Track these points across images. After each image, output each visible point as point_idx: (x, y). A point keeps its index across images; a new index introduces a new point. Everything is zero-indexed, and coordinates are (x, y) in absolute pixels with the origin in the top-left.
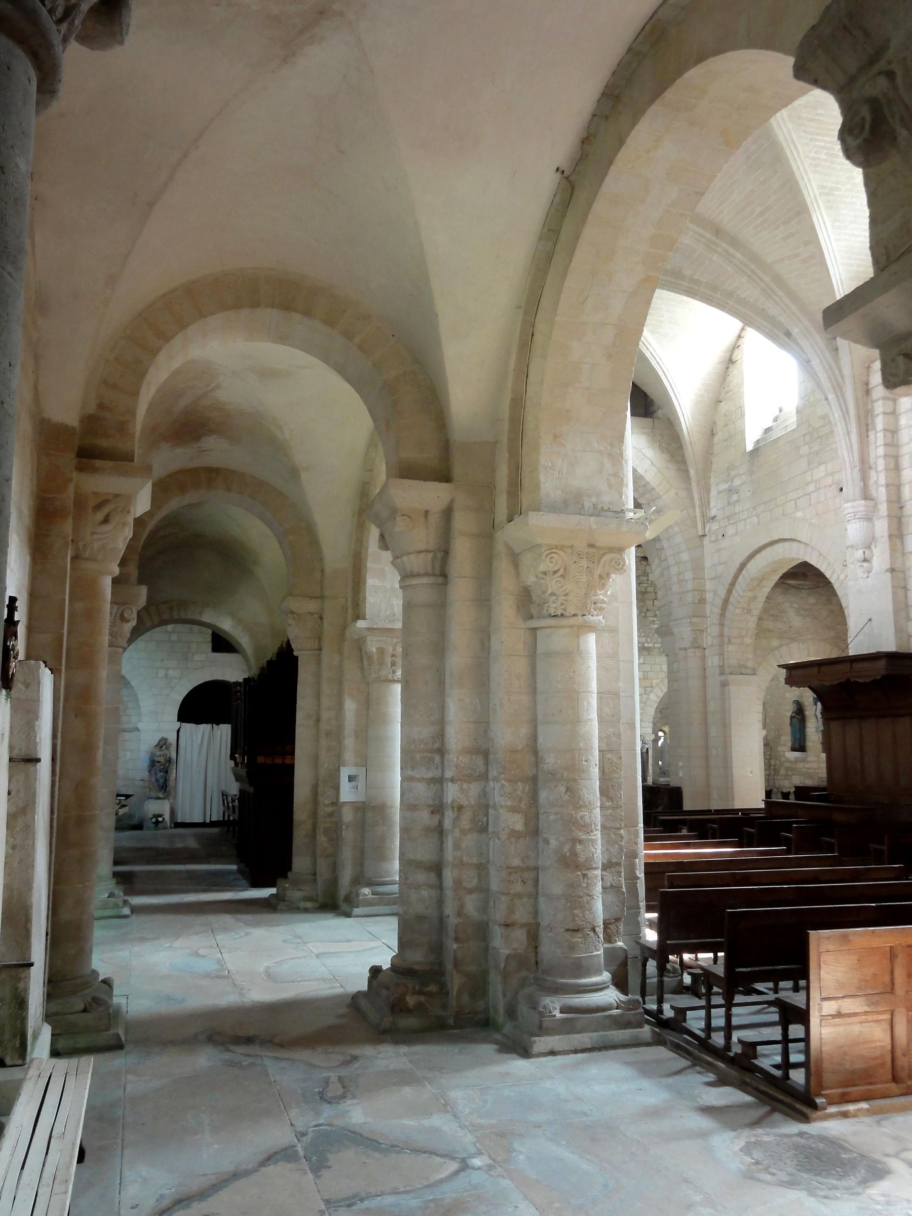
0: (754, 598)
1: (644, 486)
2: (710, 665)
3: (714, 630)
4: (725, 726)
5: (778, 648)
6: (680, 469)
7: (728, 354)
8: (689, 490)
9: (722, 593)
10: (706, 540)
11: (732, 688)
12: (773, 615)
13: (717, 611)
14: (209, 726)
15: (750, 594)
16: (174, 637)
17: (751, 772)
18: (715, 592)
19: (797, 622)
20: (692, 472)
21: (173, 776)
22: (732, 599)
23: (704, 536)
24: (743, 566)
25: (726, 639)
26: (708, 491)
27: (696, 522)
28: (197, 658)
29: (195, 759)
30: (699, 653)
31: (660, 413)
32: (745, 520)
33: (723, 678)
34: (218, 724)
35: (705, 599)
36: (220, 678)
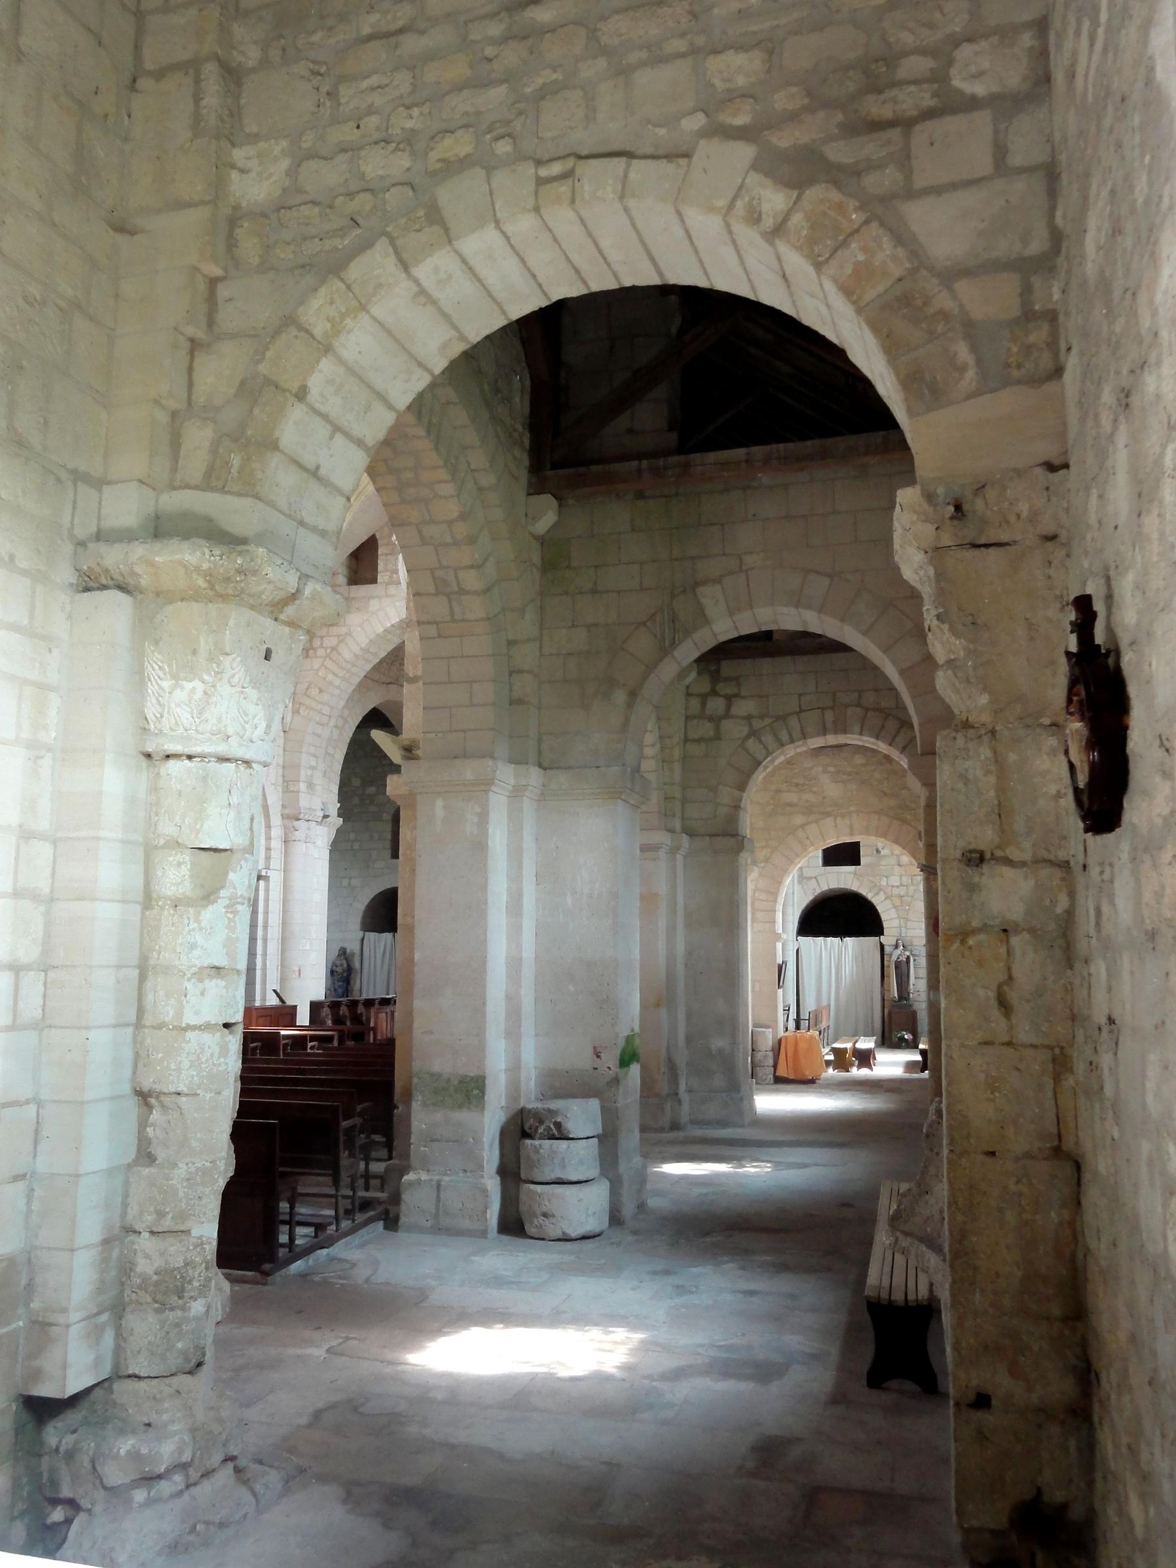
5: (803, 826)
12: (797, 785)
16: (356, 847)
19: (833, 790)
21: (357, 986)
28: (378, 865)
29: (378, 969)
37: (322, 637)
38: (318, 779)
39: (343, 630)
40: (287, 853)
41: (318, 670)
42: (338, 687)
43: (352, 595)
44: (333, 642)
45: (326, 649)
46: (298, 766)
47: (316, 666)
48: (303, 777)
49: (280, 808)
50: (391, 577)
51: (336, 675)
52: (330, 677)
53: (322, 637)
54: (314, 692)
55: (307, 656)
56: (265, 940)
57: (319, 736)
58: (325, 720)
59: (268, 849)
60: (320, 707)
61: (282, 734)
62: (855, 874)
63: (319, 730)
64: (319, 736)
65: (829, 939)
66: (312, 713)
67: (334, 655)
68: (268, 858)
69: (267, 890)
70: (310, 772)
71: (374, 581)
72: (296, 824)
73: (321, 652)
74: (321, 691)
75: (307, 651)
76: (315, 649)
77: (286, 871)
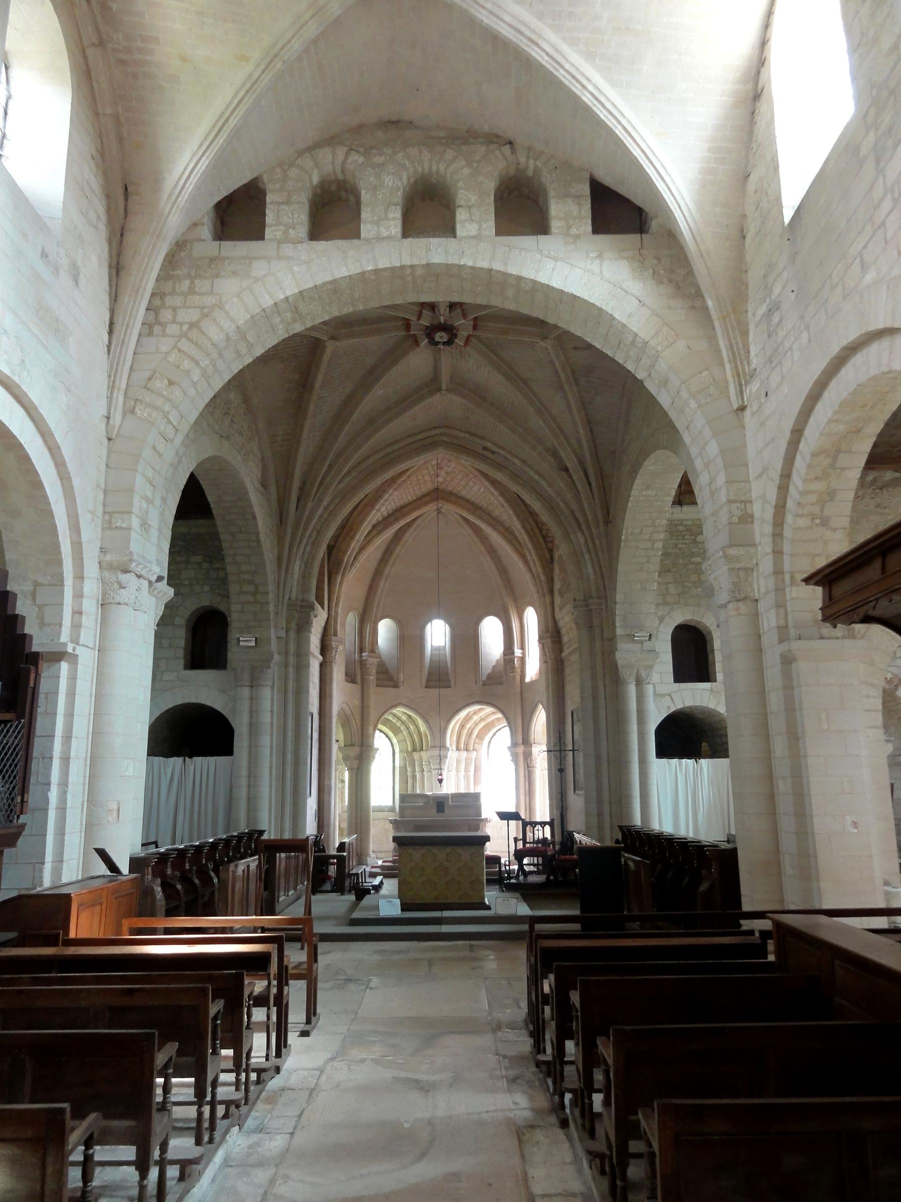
0: (831, 494)
1: (633, 343)
2: (766, 628)
3: (767, 565)
4: (794, 736)
6: (693, 307)
7: (750, 86)
8: (712, 339)
9: (772, 495)
10: (747, 413)
11: (802, 667)
13: (768, 529)
14: (181, 759)
15: (819, 486)
17: (855, 825)
18: (763, 497)
20: (710, 303)
22: (790, 504)
23: (742, 409)
24: (797, 433)
25: (787, 577)
26: (745, 333)
27: (727, 387)
29: (162, 804)
30: (743, 607)
31: (654, 225)
32: (790, 349)
33: (783, 648)
34: (191, 757)
35: (752, 516)
36: (193, 700)
37: (174, 309)
38: (154, 521)
39: (210, 300)
40: (104, 622)
41: (168, 353)
42: (194, 384)
43: (224, 253)
44: (194, 315)
45: (181, 324)
46: (130, 491)
47: (164, 349)
48: (136, 510)
49: (96, 552)
50: (286, 233)
51: (197, 363)
52: (187, 364)
53: (174, 309)
54: (159, 384)
55: (150, 334)
56: (66, 760)
57: (160, 455)
58: (170, 431)
59: (78, 612)
60: (167, 407)
61: (106, 441)
62: (712, 690)
63: (161, 447)
64: (160, 455)
65: (684, 760)
66: (154, 414)
67: (194, 334)
68: (76, 627)
69: (73, 678)
70: (144, 505)
71: (260, 236)
72: (123, 577)
73: (172, 329)
74: (171, 383)
75: (151, 327)
76: (163, 325)
77: (102, 650)
